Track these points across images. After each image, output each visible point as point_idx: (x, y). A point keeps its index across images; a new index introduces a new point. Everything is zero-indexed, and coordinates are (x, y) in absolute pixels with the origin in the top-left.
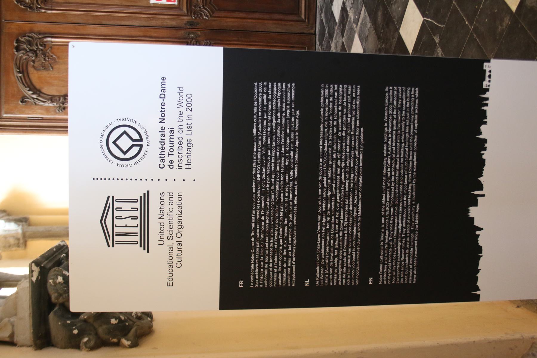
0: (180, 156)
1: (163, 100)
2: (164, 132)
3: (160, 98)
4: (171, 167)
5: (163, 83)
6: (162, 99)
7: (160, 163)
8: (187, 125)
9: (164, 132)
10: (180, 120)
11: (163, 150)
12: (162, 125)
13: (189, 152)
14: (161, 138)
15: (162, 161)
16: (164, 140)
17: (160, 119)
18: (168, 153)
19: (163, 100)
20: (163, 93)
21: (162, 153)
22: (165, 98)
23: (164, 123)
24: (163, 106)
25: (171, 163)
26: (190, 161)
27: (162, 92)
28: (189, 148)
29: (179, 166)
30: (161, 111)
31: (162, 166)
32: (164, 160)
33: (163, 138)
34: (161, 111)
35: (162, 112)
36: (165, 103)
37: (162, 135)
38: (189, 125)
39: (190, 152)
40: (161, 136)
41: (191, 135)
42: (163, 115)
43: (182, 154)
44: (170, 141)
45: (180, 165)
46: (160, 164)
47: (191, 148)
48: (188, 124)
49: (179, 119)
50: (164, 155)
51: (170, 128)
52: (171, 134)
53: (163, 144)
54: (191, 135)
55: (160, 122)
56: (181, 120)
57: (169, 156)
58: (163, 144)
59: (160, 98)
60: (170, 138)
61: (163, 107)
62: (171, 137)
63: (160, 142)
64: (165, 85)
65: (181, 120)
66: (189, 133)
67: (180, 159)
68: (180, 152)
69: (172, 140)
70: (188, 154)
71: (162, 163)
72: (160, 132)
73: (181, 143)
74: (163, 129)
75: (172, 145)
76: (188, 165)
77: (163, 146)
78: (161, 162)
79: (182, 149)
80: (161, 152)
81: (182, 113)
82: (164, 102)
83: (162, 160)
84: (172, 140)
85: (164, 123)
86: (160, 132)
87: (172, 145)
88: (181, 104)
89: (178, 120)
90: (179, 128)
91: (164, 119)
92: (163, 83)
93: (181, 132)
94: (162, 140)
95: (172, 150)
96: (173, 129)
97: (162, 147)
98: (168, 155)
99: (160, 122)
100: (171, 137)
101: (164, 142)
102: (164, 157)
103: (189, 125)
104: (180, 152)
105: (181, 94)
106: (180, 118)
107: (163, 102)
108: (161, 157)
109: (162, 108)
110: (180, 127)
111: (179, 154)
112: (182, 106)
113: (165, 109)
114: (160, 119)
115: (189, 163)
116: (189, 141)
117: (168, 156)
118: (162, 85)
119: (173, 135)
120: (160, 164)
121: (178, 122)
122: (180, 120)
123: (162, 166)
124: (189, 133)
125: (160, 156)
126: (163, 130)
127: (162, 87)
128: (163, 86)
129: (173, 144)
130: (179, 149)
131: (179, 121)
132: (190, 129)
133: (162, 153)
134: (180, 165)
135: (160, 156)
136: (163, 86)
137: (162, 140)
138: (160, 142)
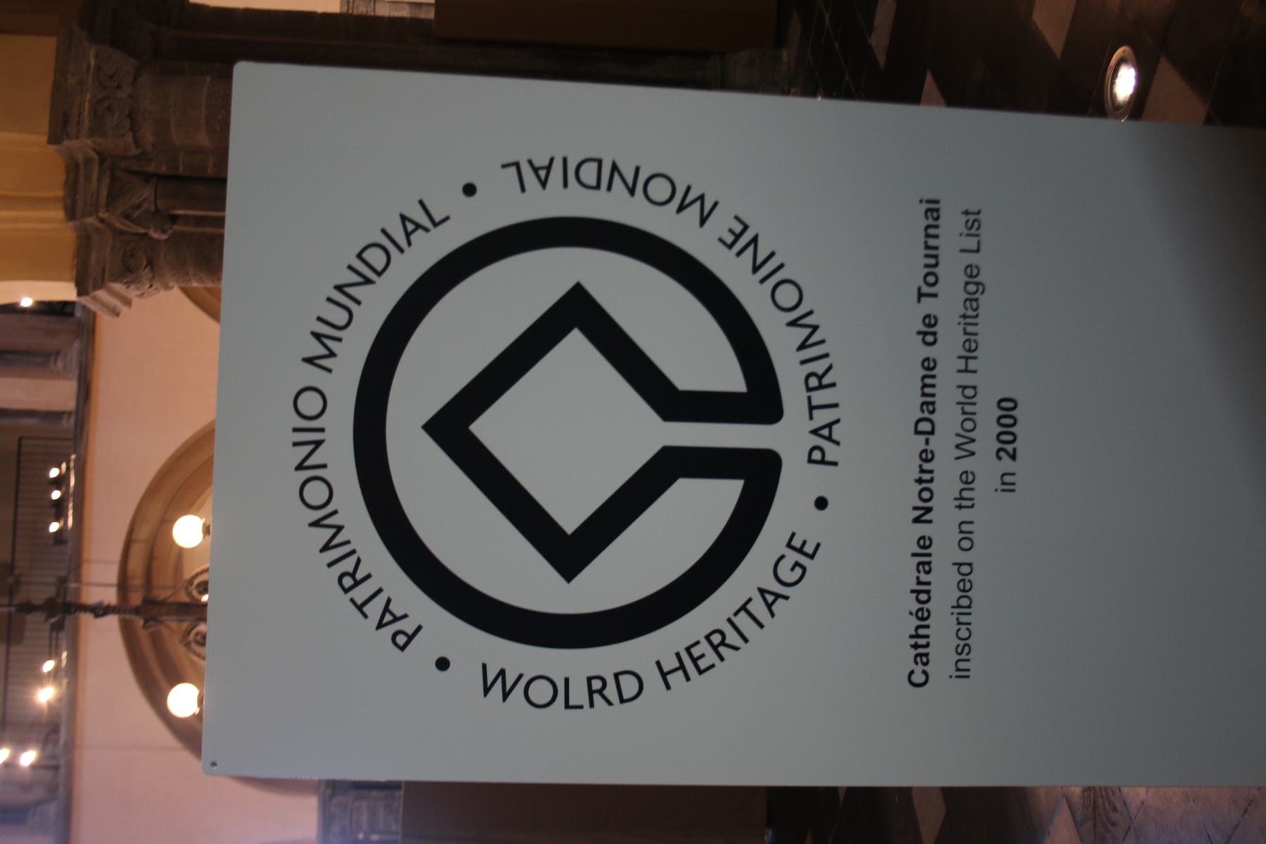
0: (964, 634)
1: (927, 442)
2: (929, 555)
3: (917, 432)
4: (930, 339)
5: (928, 381)
6: (923, 438)
7: (913, 666)
8: (964, 218)
9: (929, 555)
10: (964, 503)
11: (922, 619)
12: (922, 529)
13: (970, 313)
14: (918, 578)
15: (918, 659)
16: (929, 583)
17: (915, 508)
18: (919, 289)
19: (927, 442)
20: (926, 415)
21: (921, 632)
22: (932, 432)
23: (930, 522)
24: (927, 461)
25: (930, 325)
26: (973, 346)
27: (923, 411)
28: (971, 300)
29: (958, 670)
30: (920, 481)
31: (917, 678)
32: (927, 655)
33: (924, 578)
34: (920, 481)
35: (924, 485)
36: (932, 452)
37: (921, 567)
38: (972, 218)
39: (974, 314)
40: (919, 571)
41: (978, 251)
42: (926, 495)
43: (968, 626)
44: (927, 247)
45: (962, 665)
46: (912, 672)
47: (976, 300)
48: (966, 213)
49: (962, 498)
50: (927, 637)
51: (929, 201)
52: (931, 222)
53: (923, 597)
54: (978, 251)
55: (917, 520)
56: (969, 503)
57: (923, 299)
58: (923, 597)
59: (917, 432)
60: (928, 236)
61: (926, 466)
62: (931, 231)
63: (913, 591)
64: (933, 386)
65: (969, 503)
66: (971, 243)
67: (962, 643)
68: (963, 619)
69: (932, 242)
70: (968, 320)
71: (920, 668)
72: (914, 555)
73: (968, 586)
74: (925, 543)
75: (932, 261)
76: (967, 358)
77: (925, 606)
78: (916, 663)
79: (969, 607)
80: (918, 627)
81: (970, 478)
82: (929, 448)
83: (921, 655)
84: (932, 242)
85: (930, 522)
86: (914, 555)
87: (932, 261)
88: (970, 447)
89: (957, 503)
90: (961, 532)
91: (929, 510)
92: (928, 381)
93: (966, 544)
94: (919, 583)
95: (931, 279)
96: (937, 202)
97: (921, 609)
98: (921, 295)
99: (917, 520)
100: (931, 231)
101: (928, 592)
102: (927, 645)
103: (972, 218)
104: (963, 619)
105: (968, 408)
106: (965, 494)
107: (925, 447)
108: (915, 646)
109: (922, 471)
110: (965, 527)
111: (959, 623)
112: (973, 454)
113: (931, 472)
114: (915, 508)
115: (970, 351)
116: (972, 273)
117: (919, 301)
118: (924, 386)
119: (937, 227)
120: (912, 672)
121: (957, 509)
122: (964, 503)
123: (917, 678)
124: (971, 243)
125: (913, 641)
126: (924, 547)
127: (924, 395)
128: (927, 390)
129: (936, 257)
130: (959, 606)
131: (960, 507)
132: (973, 231)
133: (921, 632)
134: (962, 665)
135: (913, 641)
136: (927, 390)
137: (919, 583)
138: (913, 591)
